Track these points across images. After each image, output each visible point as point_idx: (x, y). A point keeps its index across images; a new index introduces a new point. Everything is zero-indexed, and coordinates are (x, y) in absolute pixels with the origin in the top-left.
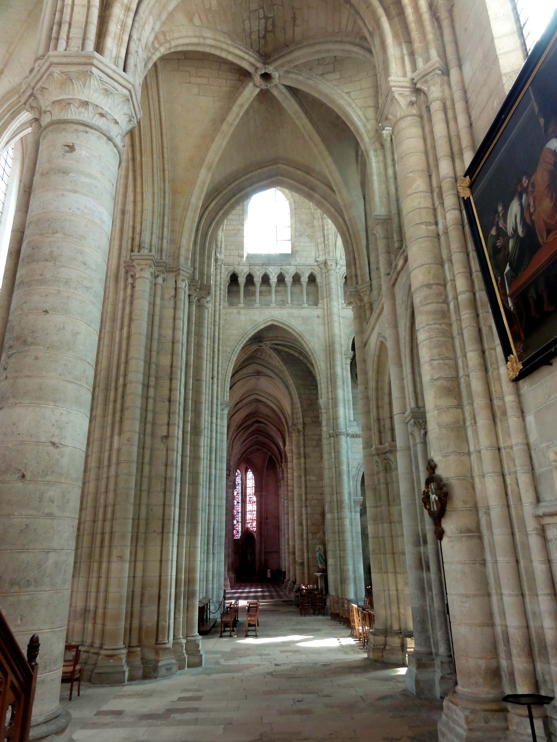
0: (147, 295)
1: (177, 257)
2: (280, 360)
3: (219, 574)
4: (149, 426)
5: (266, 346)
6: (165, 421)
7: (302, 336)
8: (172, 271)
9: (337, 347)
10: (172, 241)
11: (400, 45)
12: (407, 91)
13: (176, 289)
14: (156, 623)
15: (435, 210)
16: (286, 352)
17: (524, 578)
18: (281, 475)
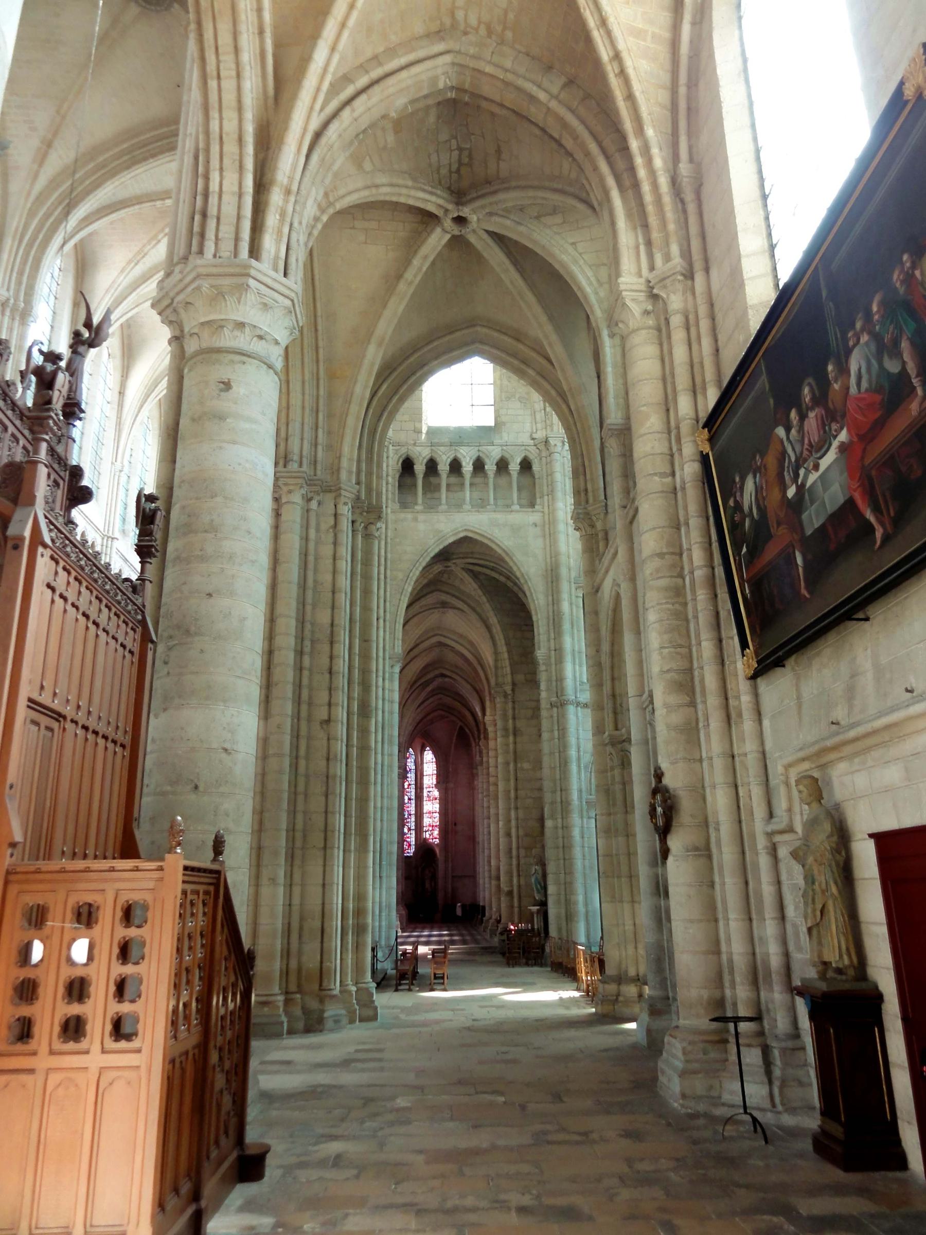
0: (297, 528)
1: (335, 470)
4: (304, 708)
5: (456, 567)
6: (326, 699)
8: (330, 491)
9: (564, 571)
10: (329, 447)
11: (635, 228)
12: (642, 296)
13: (336, 515)
14: (318, 964)
15: (672, 455)
16: (486, 575)
17: (752, 900)
18: (478, 758)
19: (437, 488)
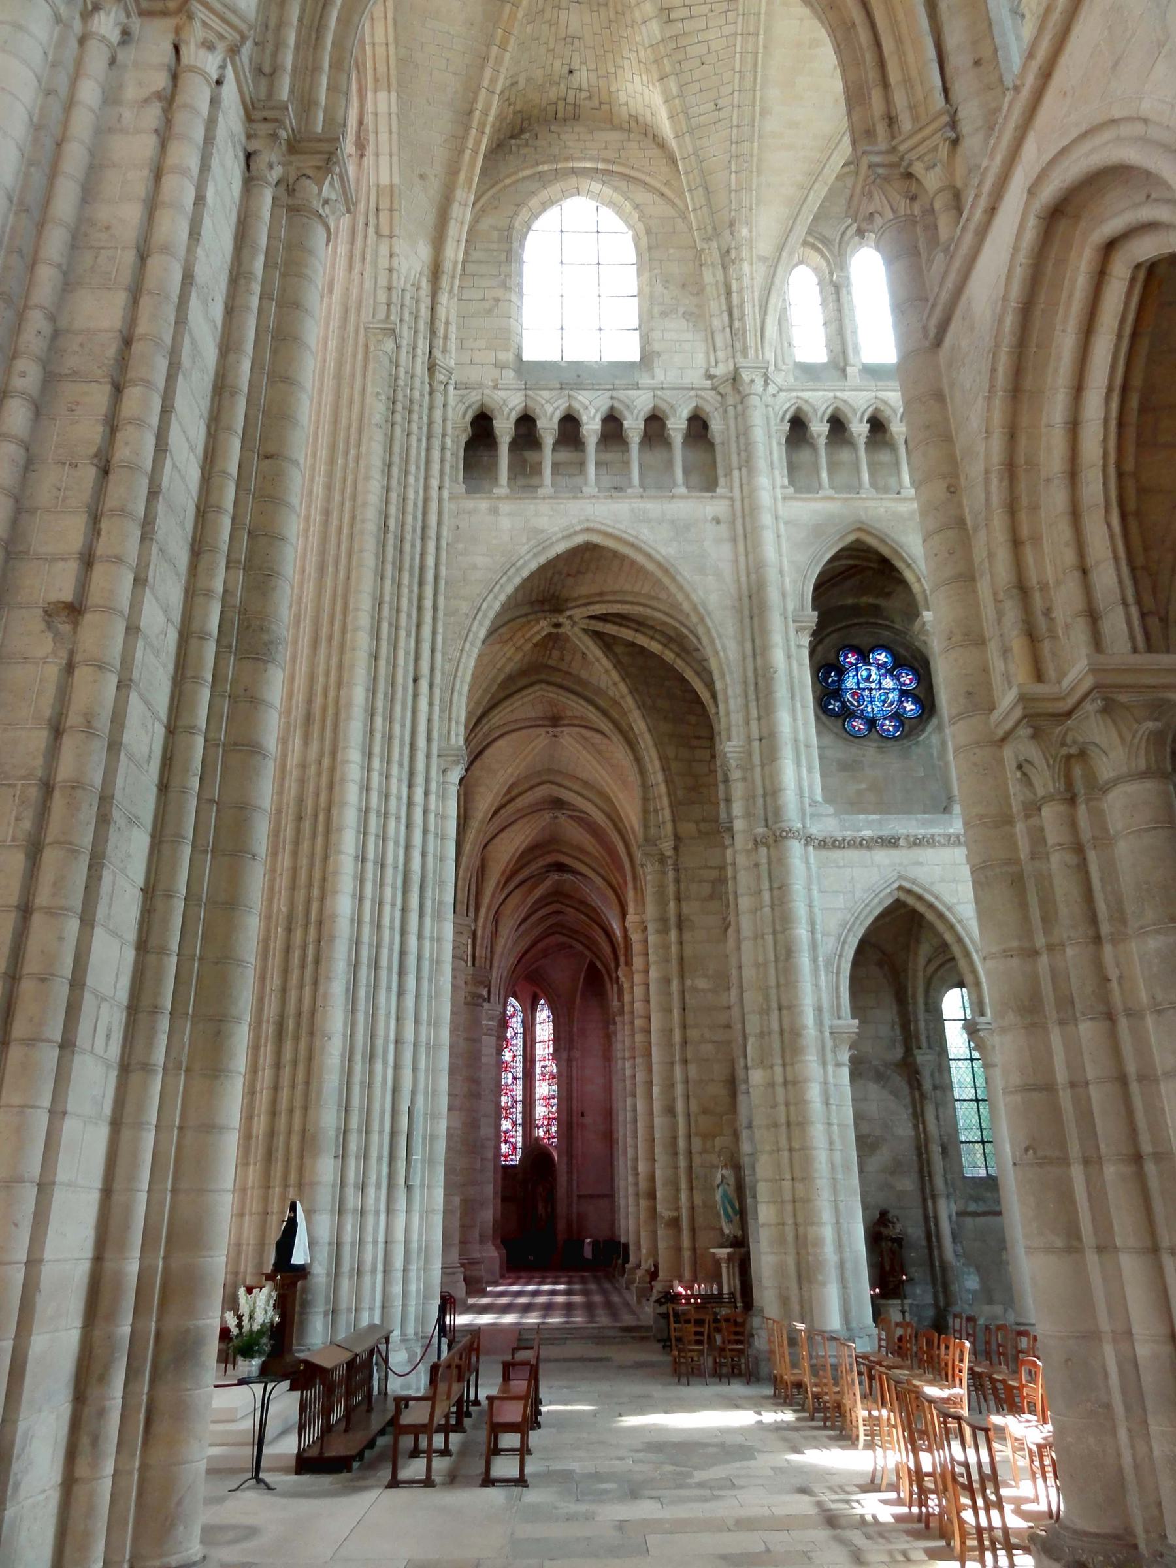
2: (609, 666)
3: (426, 1250)
7: (672, 570)
9: (773, 595)
18: (616, 1003)
19: (536, 470)
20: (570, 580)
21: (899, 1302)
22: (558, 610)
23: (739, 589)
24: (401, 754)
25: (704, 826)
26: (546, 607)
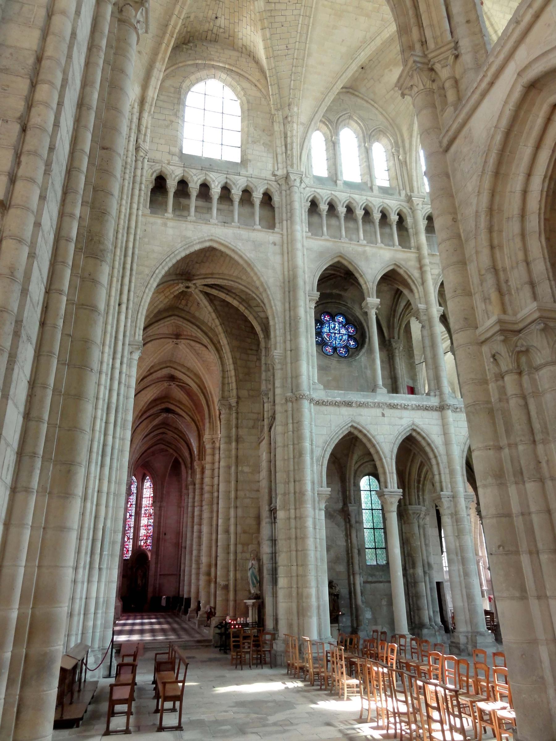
3: (107, 602)
7: (252, 265)
9: (300, 282)
19: (187, 208)
20: (198, 265)
21: (337, 625)
22: (189, 280)
23: (284, 278)
24: (110, 341)
25: (251, 393)
26: (183, 278)
